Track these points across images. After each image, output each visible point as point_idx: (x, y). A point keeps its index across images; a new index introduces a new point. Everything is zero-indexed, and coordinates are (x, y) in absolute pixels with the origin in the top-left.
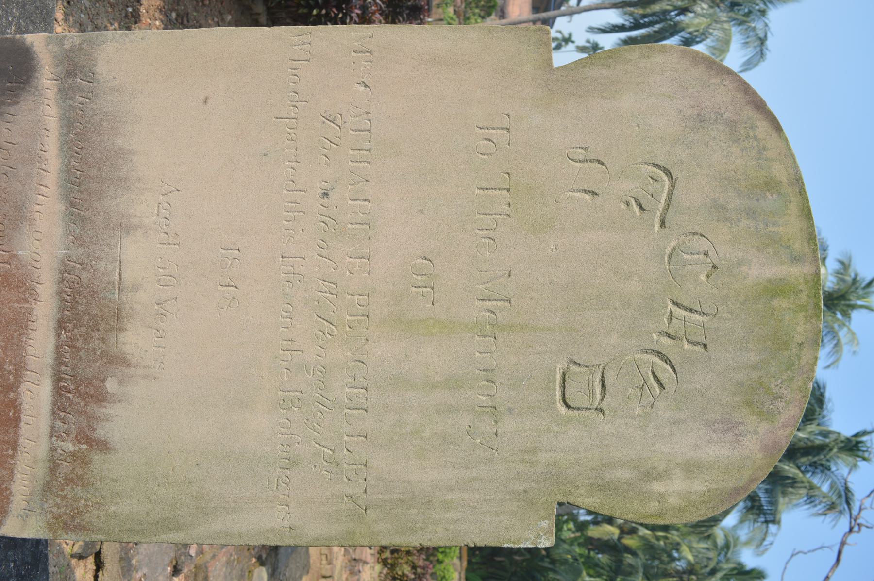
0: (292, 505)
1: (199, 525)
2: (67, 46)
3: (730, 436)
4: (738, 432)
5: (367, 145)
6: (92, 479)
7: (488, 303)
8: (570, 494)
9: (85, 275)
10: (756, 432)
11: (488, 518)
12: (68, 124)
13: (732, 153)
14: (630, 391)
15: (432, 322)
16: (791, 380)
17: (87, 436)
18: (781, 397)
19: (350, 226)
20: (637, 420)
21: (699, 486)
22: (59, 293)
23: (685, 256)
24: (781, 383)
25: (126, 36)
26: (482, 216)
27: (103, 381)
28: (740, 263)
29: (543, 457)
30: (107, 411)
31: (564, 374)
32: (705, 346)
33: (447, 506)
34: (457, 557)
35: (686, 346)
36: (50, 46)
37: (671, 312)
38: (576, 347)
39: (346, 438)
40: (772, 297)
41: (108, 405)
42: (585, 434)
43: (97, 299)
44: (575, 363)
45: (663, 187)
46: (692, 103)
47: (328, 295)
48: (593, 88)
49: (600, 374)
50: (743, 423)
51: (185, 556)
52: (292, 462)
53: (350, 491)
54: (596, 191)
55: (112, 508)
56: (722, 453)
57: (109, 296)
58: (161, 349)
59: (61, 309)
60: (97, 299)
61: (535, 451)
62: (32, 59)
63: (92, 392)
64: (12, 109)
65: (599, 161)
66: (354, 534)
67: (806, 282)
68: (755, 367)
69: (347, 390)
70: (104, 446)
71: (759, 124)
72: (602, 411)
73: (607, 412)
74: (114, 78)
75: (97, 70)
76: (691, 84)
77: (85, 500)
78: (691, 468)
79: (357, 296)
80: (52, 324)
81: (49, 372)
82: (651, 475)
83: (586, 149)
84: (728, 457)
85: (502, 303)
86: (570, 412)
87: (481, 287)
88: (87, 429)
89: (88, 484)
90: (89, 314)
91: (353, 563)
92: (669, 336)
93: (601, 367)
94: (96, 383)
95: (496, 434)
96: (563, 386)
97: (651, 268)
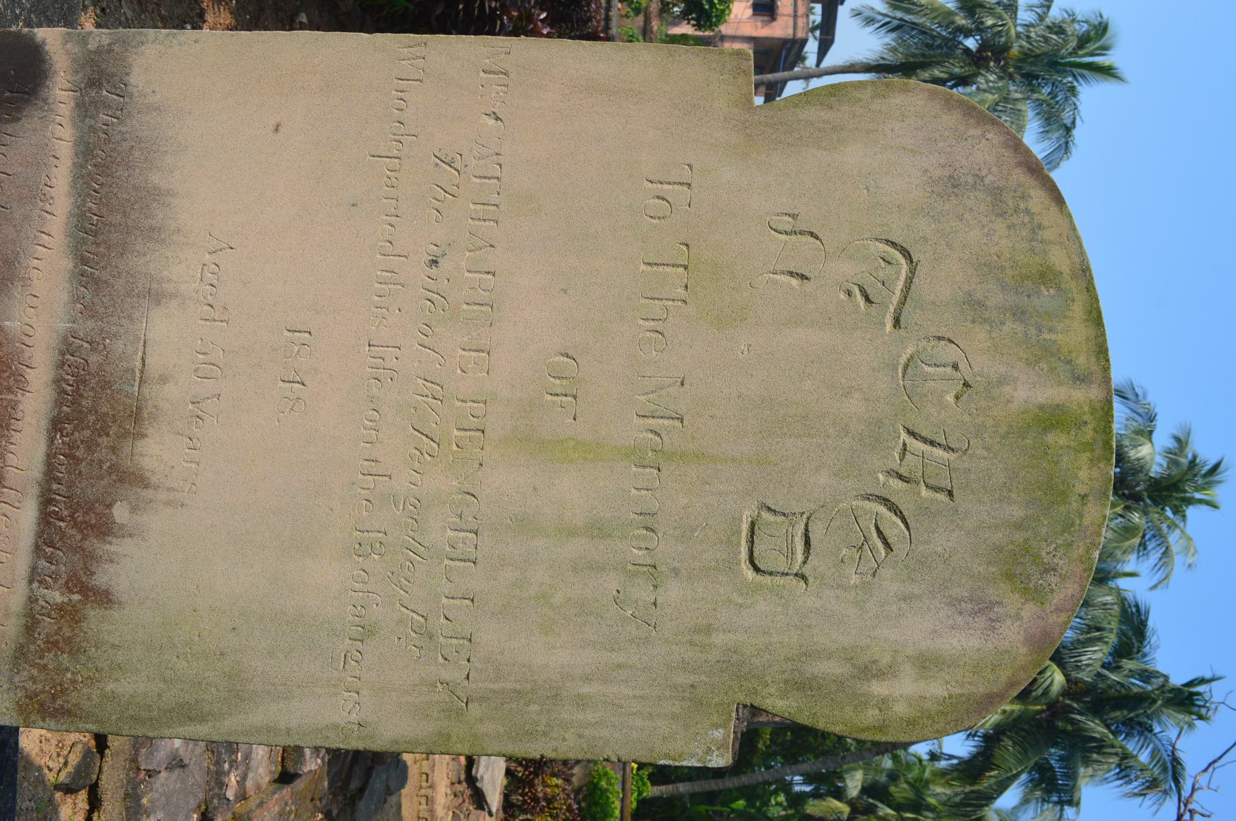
0: (363, 692)
1: (231, 715)
2: (92, 46)
3: (981, 621)
4: (993, 616)
5: (494, 198)
6: (84, 644)
7: (651, 421)
8: (756, 693)
9: (94, 359)
10: (1018, 617)
11: (639, 722)
12: (85, 150)
13: (995, 231)
14: (844, 551)
15: (572, 443)
16: (1069, 545)
17: (82, 582)
18: (1054, 570)
19: (465, 306)
20: (853, 592)
22: (57, 381)
23: (926, 368)
24: (1055, 549)
25: (174, 36)
26: (648, 301)
27: (110, 506)
28: (1001, 381)
29: (719, 639)
30: (113, 548)
31: (753, 524)
32: (950, 493)
33: (581, 702)
35: (924, 492)
36: (69, 46)
37: (904, 444)
38: (771, 487)
39: (444, 600)
40: (1045, 430)
41: (114, 540)
42: (779, 609)
43: (109, 392)
44: (769, 509)
45: (898, 273)
46: (942, 161)
47: (430, 400)
48: (807, 134)
49: (803, 527)
50: (1000, 603)
51: (220, 799)
52: (367, 632)
53: (446, 676)
54: (807, 274)
55: (110, 686)
56: (970, 644)
57: (126, 388)
58: (193, 465)
59: (58, 403)
60: (109, 392)
61: (709, 629)
62: (43, 61)
63: (93, 522)
64: (10, 128)
65: (812, 234)
66: (449, 737)
67: (1093, 411)
68: (1019, 526)
69: (450, 533)
70: (105, 598)
71: (1033, 193)
72: (803, 577)
73: (811, 580)
74: (154, 92)
75: (132, 81)
76: (941, 136)
77: (73, 673)
78: (927, 663)
79: (470, 404)
80: (44, 424)
81: (35, 491)
82: (869, 671)
83: (794, 216)
84: (978, 650)
85: (671, 422)
86: (759, 578)
87: (642, 398)
88: (82, 572)
89: (78, 650)
90: (96, 412)
92: (900, 477)
93: (805, 516)
94: (99, 508)
95: (655, 604)
96: (751, 542)
97: (878, 382)
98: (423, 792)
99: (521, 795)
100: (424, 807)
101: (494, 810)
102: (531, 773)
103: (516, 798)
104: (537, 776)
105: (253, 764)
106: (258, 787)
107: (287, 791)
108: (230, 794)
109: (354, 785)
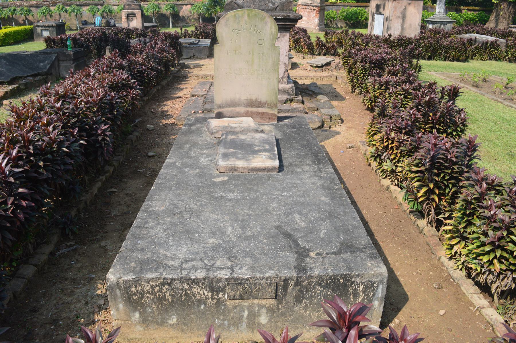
12: (227, 107)
21: (273, 27)
33: (274, 59)
34: (365, 9)
52: (269, 78)
70: (267, 101)
78: (271, 28)
82: (272, 33)
91: (337, 68)
98: (321, 79)
99: (331, 50)
101: (333, 59)
103: (332, 52)
107: (305, 102)
108: (302, 109)
109: (311, 93)
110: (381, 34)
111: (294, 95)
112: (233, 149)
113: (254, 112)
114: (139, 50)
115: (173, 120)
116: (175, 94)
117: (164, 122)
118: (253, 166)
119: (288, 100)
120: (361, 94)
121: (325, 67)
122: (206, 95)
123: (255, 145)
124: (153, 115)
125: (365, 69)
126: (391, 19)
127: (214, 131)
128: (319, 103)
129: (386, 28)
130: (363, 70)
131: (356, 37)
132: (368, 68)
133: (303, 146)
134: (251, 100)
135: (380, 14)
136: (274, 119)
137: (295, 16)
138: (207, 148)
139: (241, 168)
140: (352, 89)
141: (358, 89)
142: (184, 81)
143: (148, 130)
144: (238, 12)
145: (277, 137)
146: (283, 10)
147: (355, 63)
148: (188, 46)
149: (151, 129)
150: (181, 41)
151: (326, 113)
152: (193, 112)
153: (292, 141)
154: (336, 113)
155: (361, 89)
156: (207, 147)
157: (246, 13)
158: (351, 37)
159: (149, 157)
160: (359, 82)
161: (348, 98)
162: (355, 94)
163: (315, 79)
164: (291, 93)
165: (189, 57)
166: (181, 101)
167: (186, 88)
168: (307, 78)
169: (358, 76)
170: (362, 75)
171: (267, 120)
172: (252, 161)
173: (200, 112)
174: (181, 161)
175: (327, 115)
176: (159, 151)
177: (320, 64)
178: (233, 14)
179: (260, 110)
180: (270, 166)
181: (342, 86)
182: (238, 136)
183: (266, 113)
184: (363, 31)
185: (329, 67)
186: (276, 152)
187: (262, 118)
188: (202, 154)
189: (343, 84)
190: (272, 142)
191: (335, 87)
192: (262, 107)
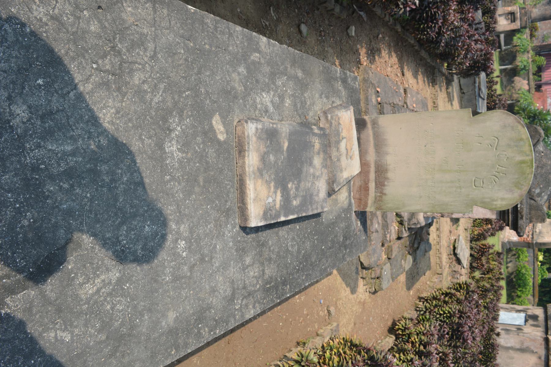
2: (373, 119)
9: (380, 163)
12: (374, 134)
16: (526, 181)
21: (504, 203)
22: (375, 166)
29: (470, 196)
33: (451, 205)
34: (531, 295)
35: (501, 174)
61: (469, 195)
68: (517, 179)
70: (385, 194)
72: (482, 187)
78: (502, 199)
81: (374, 181)
82: (493, 200)
91: (454, 273)
98: (437, 255)
99: (477, 263)
100: (438, 260)
101: (465, 266)
102: (480, 255)
103: (475, 265)
104: (482, 256)
105: (392, 233)
106: (393, 239)
107: (399, 241)
108: (388, 239)
109: (416, 246)
110: (499, 322)
111: (409, 227)
112: (288, 147)
113: (368, 177)
114: (465, 17)
115: (365, 64)
116: (408, 68)
117: (363, 52)
118: (248, 182)
119: (402, 219)
120: (416, 310)
121: (454, 258)
122: (407, 107)
123: (299, 182)
124: (374, 37)
125: (450, 317)
126: (520, 334)
127: (329, 116)
128: (399, 260)
129: (508, 328)
130: (448, 315)
131: (496, 292)
132: (452, 321)
133: (307, 257)
134: (386, 171)
135: (526, 321)
136: (359, 206)
137: (522, 227)
138: (295, 105)
139: (244, 162)
140: (423, 298)
141: (423, 307)
142: (428, 80)
143: (348, 28)
144: (527, 144)
145: (324, 216)
146: (530, 209)
147: (459, 302)
148: (477, 85)
149: (349, 31)
150: (483, 75)
151: (383, 271)
152: (379, 90)
153: (317, 239)
154: (385, 285)
155: (422, 310)
156: (299, 105)
157: (527, 158)
158: (496, 286)
159: (299, 26)
160: (432, 308)
161: (411, 293)
162: (417, 302)
163: (438, 247)
164: (412, 223)
165: (462, 87)
166: (397, 75)
167: (418, 82)
168: (439, 236)
169: (440, 306)
170: (442, 312)
171: (357, 196)
172: (260, 181)
173: (379, 99)
174: (263, 61)
175: (381, 273)
176: (312, 40)
177: (458, 251)
178: (524, 137)
179: (372, 185)
180: (249, 211)
181: (428, 283)
182: (318, 153)
183: (368, 194)
184: (504, 298)
185: (454, 263)
186: (283, 219)
187: (360, 189)
188: (282, 98)
189: (431, 284)
190: (308, 209)
191: (426, 274)
192: (377, 187)
